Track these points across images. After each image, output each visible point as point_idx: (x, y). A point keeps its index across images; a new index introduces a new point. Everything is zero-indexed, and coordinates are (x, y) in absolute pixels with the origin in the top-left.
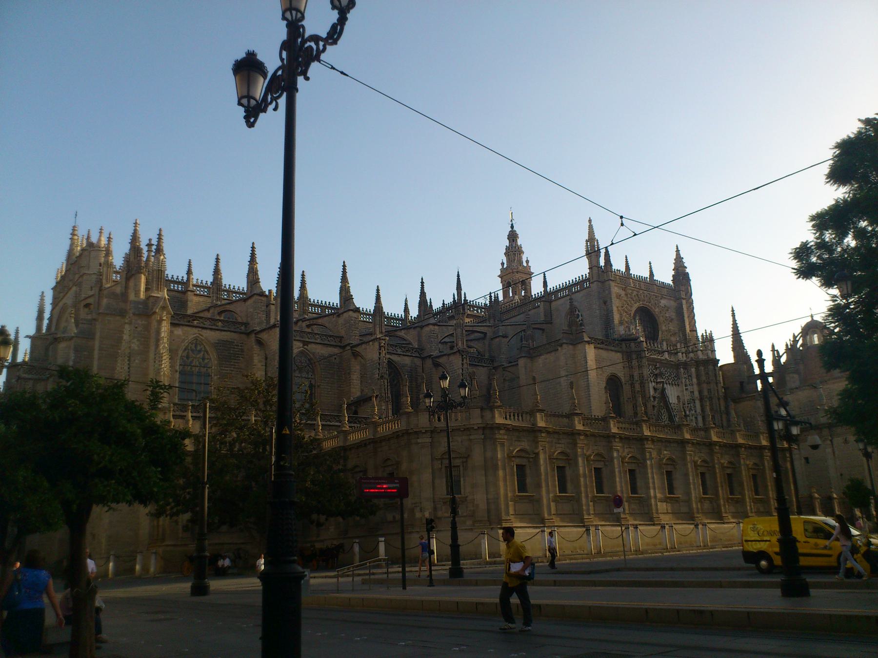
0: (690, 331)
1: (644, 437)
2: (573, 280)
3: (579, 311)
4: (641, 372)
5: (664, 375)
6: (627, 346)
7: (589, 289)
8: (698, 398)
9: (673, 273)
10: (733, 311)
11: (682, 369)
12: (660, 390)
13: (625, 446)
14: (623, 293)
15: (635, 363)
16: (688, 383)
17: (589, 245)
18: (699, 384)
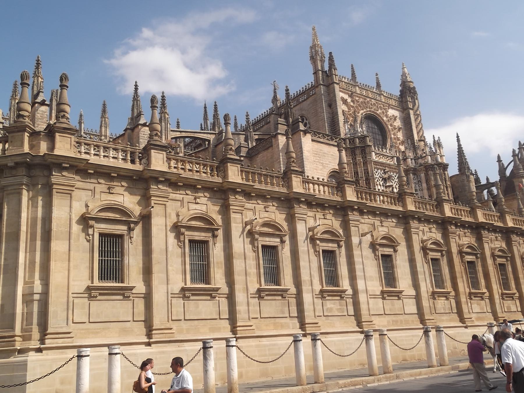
1: (347, 204)
2: (300, 91)
3: (306, 120)
4: (366, 168)
5: (394, 180)
7: (315, 95)
10: (458, 137)
11: (411, 175)
14: (349, 100)
15: (359, 159)
16: (418, 188)
17: (313, 51)
18: (429, 189)
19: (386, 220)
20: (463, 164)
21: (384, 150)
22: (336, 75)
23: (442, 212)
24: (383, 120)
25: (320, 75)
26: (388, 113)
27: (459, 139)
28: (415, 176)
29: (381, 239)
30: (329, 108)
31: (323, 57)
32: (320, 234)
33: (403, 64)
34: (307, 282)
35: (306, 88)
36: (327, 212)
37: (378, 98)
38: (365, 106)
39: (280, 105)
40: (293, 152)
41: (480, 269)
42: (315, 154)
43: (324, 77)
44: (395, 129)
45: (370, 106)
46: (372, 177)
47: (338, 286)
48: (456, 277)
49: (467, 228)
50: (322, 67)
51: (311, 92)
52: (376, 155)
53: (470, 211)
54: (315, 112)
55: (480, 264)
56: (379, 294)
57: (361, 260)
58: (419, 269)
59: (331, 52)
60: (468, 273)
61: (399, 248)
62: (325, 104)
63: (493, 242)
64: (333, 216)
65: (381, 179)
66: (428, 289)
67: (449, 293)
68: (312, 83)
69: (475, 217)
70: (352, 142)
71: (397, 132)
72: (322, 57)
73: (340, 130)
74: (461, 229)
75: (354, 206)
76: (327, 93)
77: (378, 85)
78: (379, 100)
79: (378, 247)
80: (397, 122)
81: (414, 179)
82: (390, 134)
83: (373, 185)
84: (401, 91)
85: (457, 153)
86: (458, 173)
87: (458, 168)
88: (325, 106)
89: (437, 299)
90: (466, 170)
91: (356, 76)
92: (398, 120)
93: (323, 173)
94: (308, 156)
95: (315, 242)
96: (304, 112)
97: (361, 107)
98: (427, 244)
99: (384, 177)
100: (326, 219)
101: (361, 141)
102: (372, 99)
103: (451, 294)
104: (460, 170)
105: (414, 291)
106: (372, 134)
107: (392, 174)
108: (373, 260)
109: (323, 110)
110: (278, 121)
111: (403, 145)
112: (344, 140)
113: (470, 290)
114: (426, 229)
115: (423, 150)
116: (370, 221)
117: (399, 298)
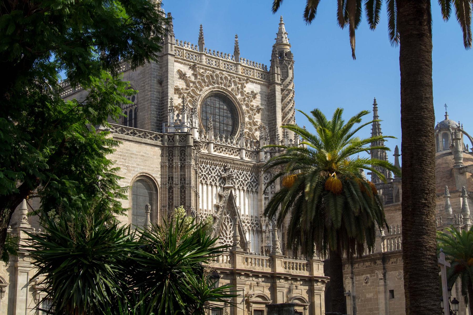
4: (183, 173)
6: (169, 139)
12: (227, 198)
14: (189, 73)
15: (177, 162)
22: (172, 44)
24: (236, 99)
30: (159, 85)
38: (211, 81)
46: (189, 185)
59: (170, 13)
63: (252, 288)
65: (219, 178)
70: (171, 140)
80: (257, 101)
90: (379, 153)
92: (258, 97)
97: (205, 82)
99: (223, 176)
101: (183, 139)
102: (224, 71)
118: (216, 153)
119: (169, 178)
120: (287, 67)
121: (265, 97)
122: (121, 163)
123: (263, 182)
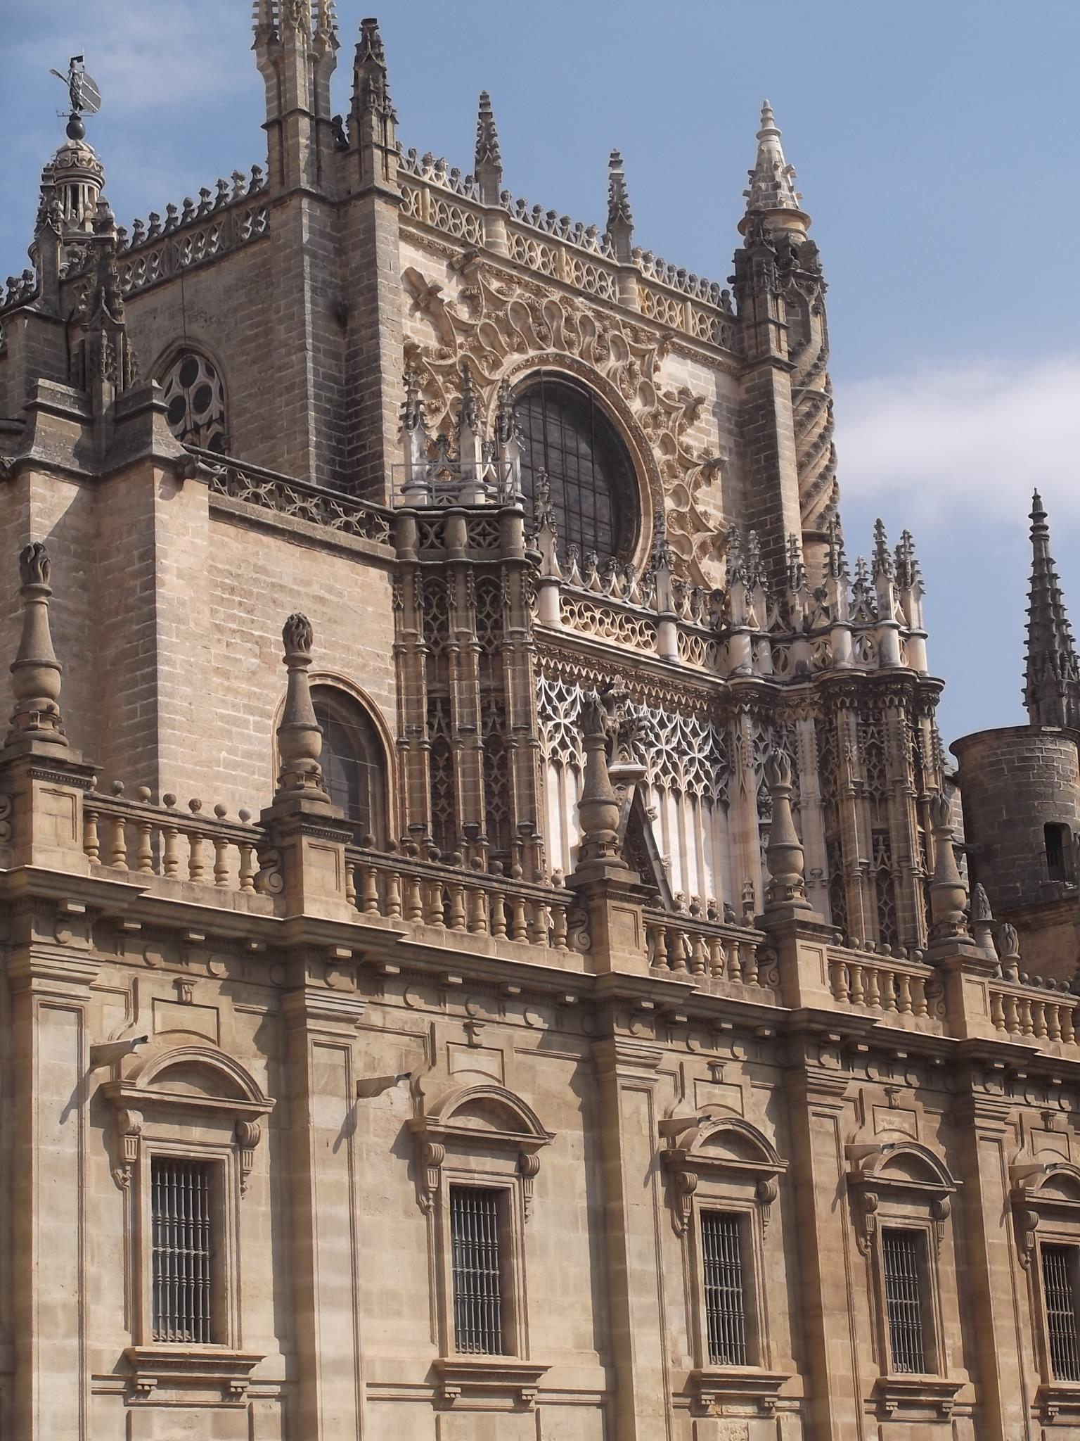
0: (808, 538)
1: (298, 936)
3: (210, 372)
4: (492, 684)
5: (651, 745)
7: (266, 245)
8: (825, 876)
9: (739, 242)
11: (747, 723)
13: (147, 991)
14: (450, 291)
18: (831, 805)
19: (496, 1017)
20: (1049, 665)
21: (616, 582)
22: (386, 152)
23: (786, 985)
24: (626, 412)
25: (303, 141)
26: (656, 377)
27: (1046, 528)
28: (766, 730)
29: (456, 1113)
30: (334, 326)
31: (325, 37)
32: (146, 1080)
33: (765, 111)
34: (60, 1314)
35: (220, 198)
36: (195, 967)
37: (611, 291)
38: (534, 328)
39: (72, 266)
40: (48, 665)
41: (945, 1269)
42: (224, 587)
43: (325, 151)
44: (687, 465)
45: (564, 332)
46: (521, 735)
47: (216, 1336)
48: (819, 1306)
49: (906, 1067)
50: (318, 93)
51: (248, 224)
52: (566, 602)
53: (929, 983)
54: (256, 336)
55: (948, 1243)
56: (422, 1383)
57: (343, 1212)
58: (633, 1264)
59: (374, 21)
60: (883, 1289)
61: (544, 1158)
62: (313, 302)
63: (1027, 1138)
64: (223, 991)
66: (670, 1364)
67: (774, 1383)
68: (255, 170)
69: (951, 1011)
70: (432, 537)
71: (697, 486)
72: (318, 40)
73: (380, 455)
74: (874, 1072)
75: (334, 946)
76: (331, 245)
77: (619, 220)
78: (615, 302)
79: (437, 1148)
80: (700, 430)
81: (761, 745)
82: (657, 494)
83: (525, 778)
84: (741, 259)
85: (1028, 604)
86: (1022, 717)
87: (1024, 683)
88: (314, 312)
89: (711, 1410)
90: (1065, 701)
91: (501, 162)
92: (707, 418)
93: (258, 697)
94: (182, 603)
95: (121, 1118)
96: (197, 329)
98: (688, 1144)
100: (190, 1004)
101: (484, 534)
102: (579, 293)
103: (783, 1390)
104: (1033, 697)
105: (602, 1371)
106: (559, 484)
107: (644, 710)
108: (407, 1213)
109: (302, 335)
110: (33, 391)
111: (719, 558)
112: (395, 519)
113: (884, 1372)
114: (696, 1066)
115: (820, 594)
116: (414, 1022)
117: (521, 1405)
118: (568, 628)
119: (432, 703)
120: (805, 304)
121: (729, 419)
122: (234, 626)
123: (752, 760)
